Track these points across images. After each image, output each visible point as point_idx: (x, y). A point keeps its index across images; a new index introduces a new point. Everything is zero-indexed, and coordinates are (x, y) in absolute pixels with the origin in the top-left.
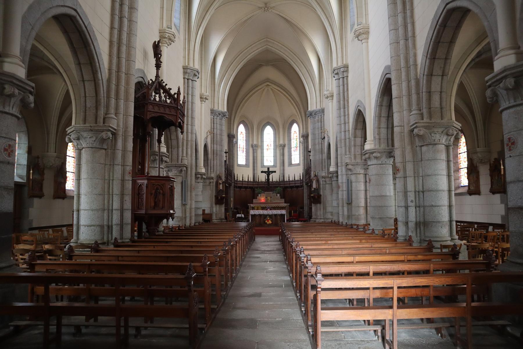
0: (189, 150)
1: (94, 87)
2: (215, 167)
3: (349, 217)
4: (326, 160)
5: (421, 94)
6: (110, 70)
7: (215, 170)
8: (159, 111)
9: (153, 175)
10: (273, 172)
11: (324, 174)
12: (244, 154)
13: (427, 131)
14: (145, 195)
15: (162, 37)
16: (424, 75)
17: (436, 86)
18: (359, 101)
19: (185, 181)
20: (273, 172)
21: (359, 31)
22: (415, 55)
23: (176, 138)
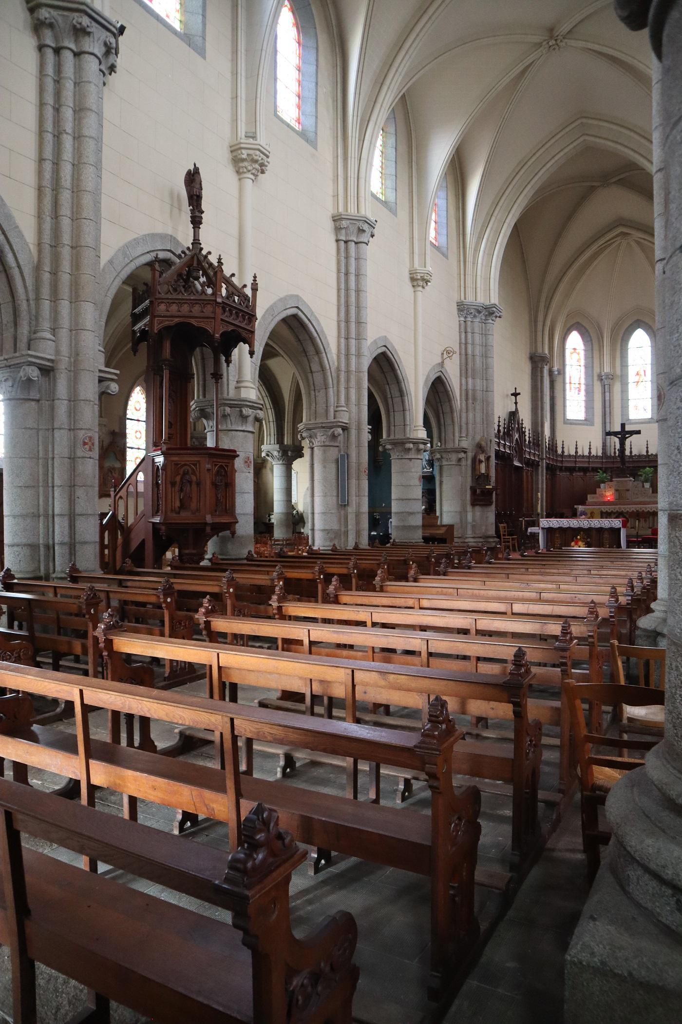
0: (353, 392)
1: (6, 284)
2: (470, 426)
9: (226, 447)
10: (632, 433)
12: (582, 396)
20: (632, 433)
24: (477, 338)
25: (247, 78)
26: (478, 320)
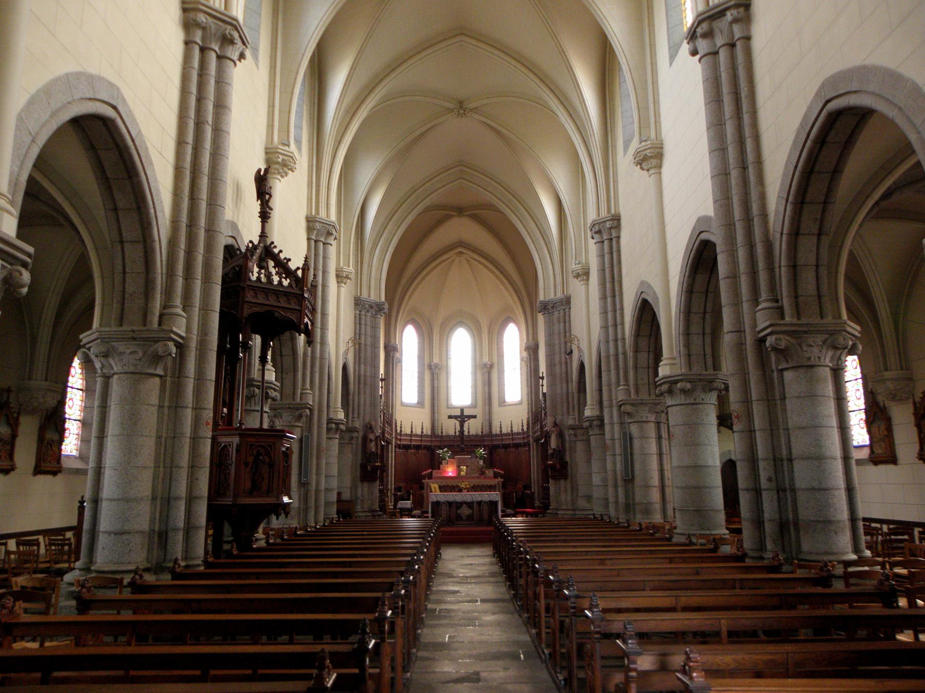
2: (362, 408)
3: (629, 507)
4: (576, 395)
5: (777, 270)
6: (175, 222)
7: (362, 415)
8: (267, 302)
9: (249, 427)
11: (571, 422)
13: (793, 341)
14: (233, 466)
15: (269, 162)
16: (782, 234)
17: (807, 254)
18: (643, 283)
19: (307, 437)
21: (644, 153)
22: (763, 197)
23: (291, 353)
24: (369, 329)
25: (281, 92)
26: (369, 314)
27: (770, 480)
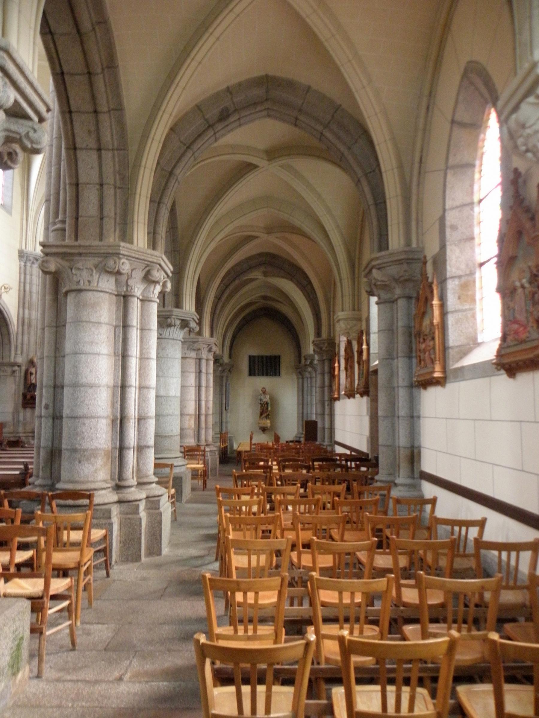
13: (66, 264)
27: (47, 407)
